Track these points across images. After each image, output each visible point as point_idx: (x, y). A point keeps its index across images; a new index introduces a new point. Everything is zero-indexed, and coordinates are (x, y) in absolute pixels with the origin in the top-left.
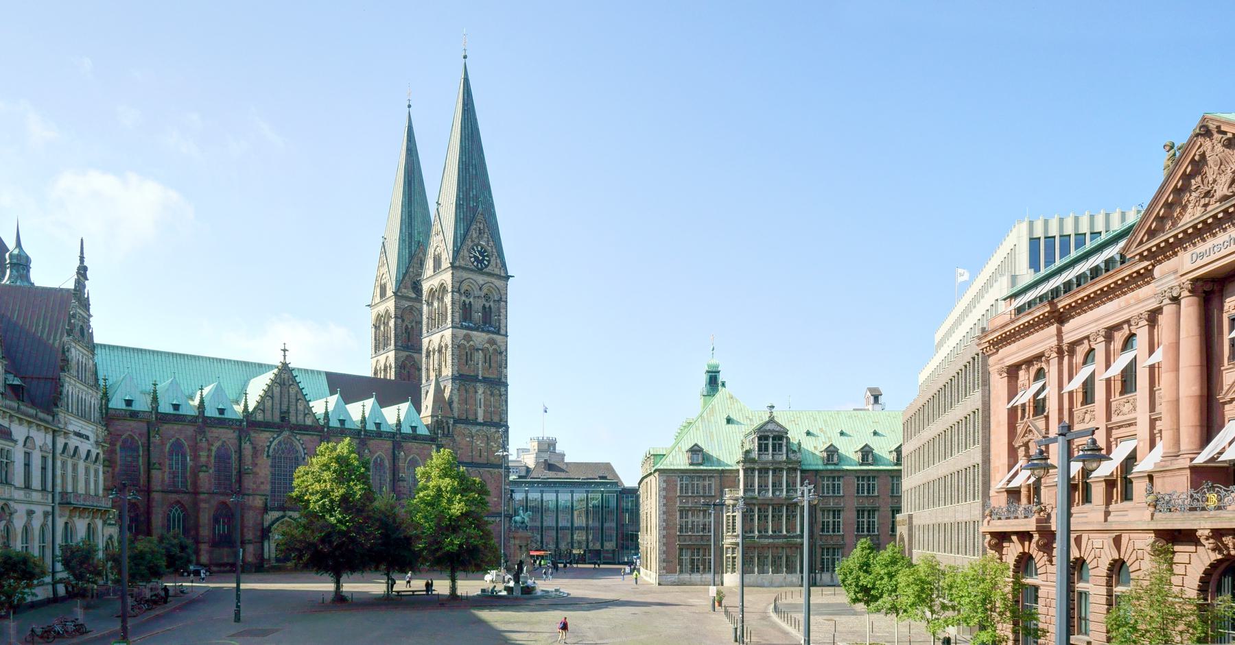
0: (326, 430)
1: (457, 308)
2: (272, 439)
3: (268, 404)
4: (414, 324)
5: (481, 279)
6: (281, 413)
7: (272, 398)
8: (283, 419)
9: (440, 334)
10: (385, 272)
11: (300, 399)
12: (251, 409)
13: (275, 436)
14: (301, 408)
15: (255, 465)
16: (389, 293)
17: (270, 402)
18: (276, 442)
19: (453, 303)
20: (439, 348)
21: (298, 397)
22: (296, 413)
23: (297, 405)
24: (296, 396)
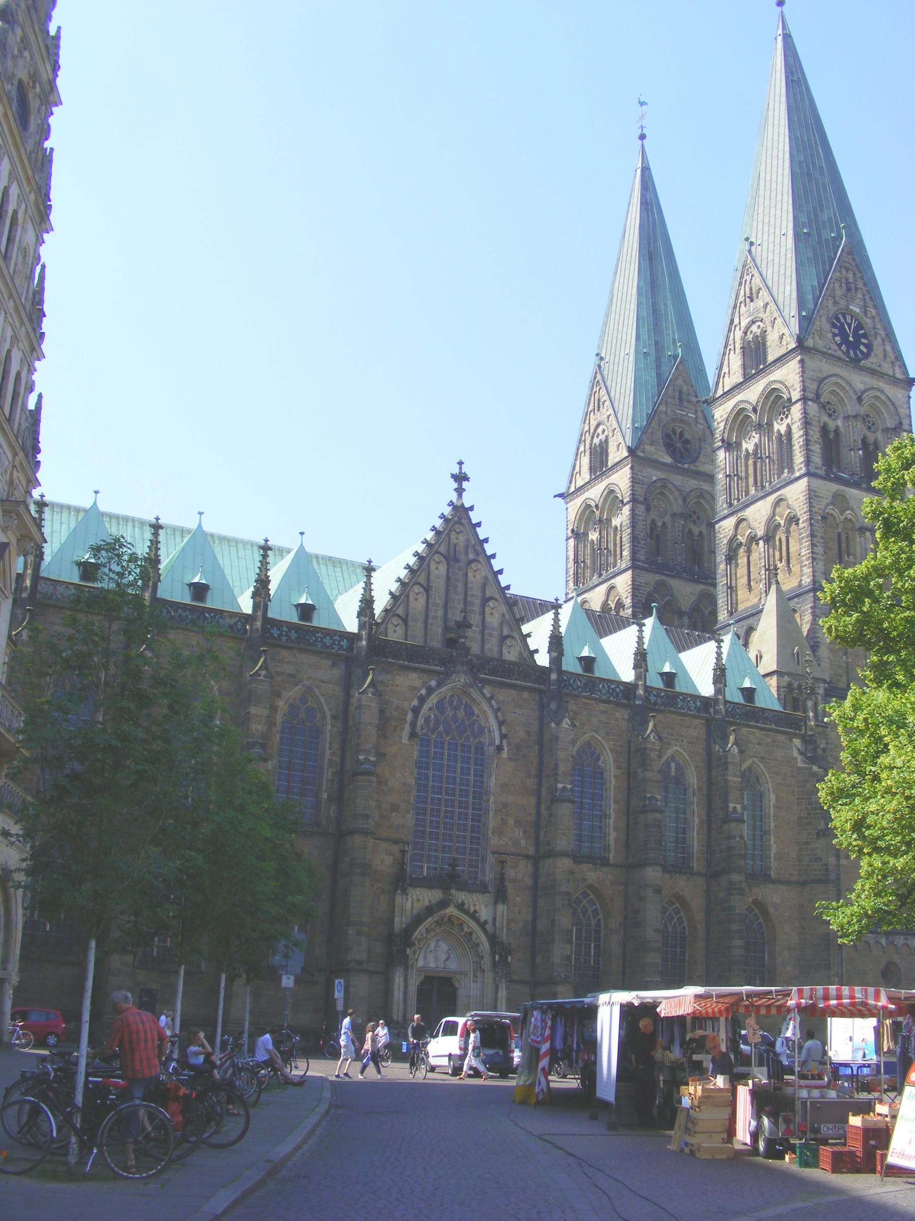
0: (554, 676)
1: (816, 435)
2: (423, 692)
3: (418, 604)
4: (667, 519)
5: (859, 381)
6: (447, 629)
7: (427, 589)
8: (451, 643)
9: (771, 499)
10: (604, 417)
11: (491, 598)
12: (379, 608)
13: (433, 683)
14: (493, 620)
15: (381, 756)
16: (617, 453)
17: (422, 600)
18: (432, 700)
19: (806, 423)
20: (767, 530)
21: (488, 594)
22: (482, 632)
23: (483, 613)
24: (484, 591)
